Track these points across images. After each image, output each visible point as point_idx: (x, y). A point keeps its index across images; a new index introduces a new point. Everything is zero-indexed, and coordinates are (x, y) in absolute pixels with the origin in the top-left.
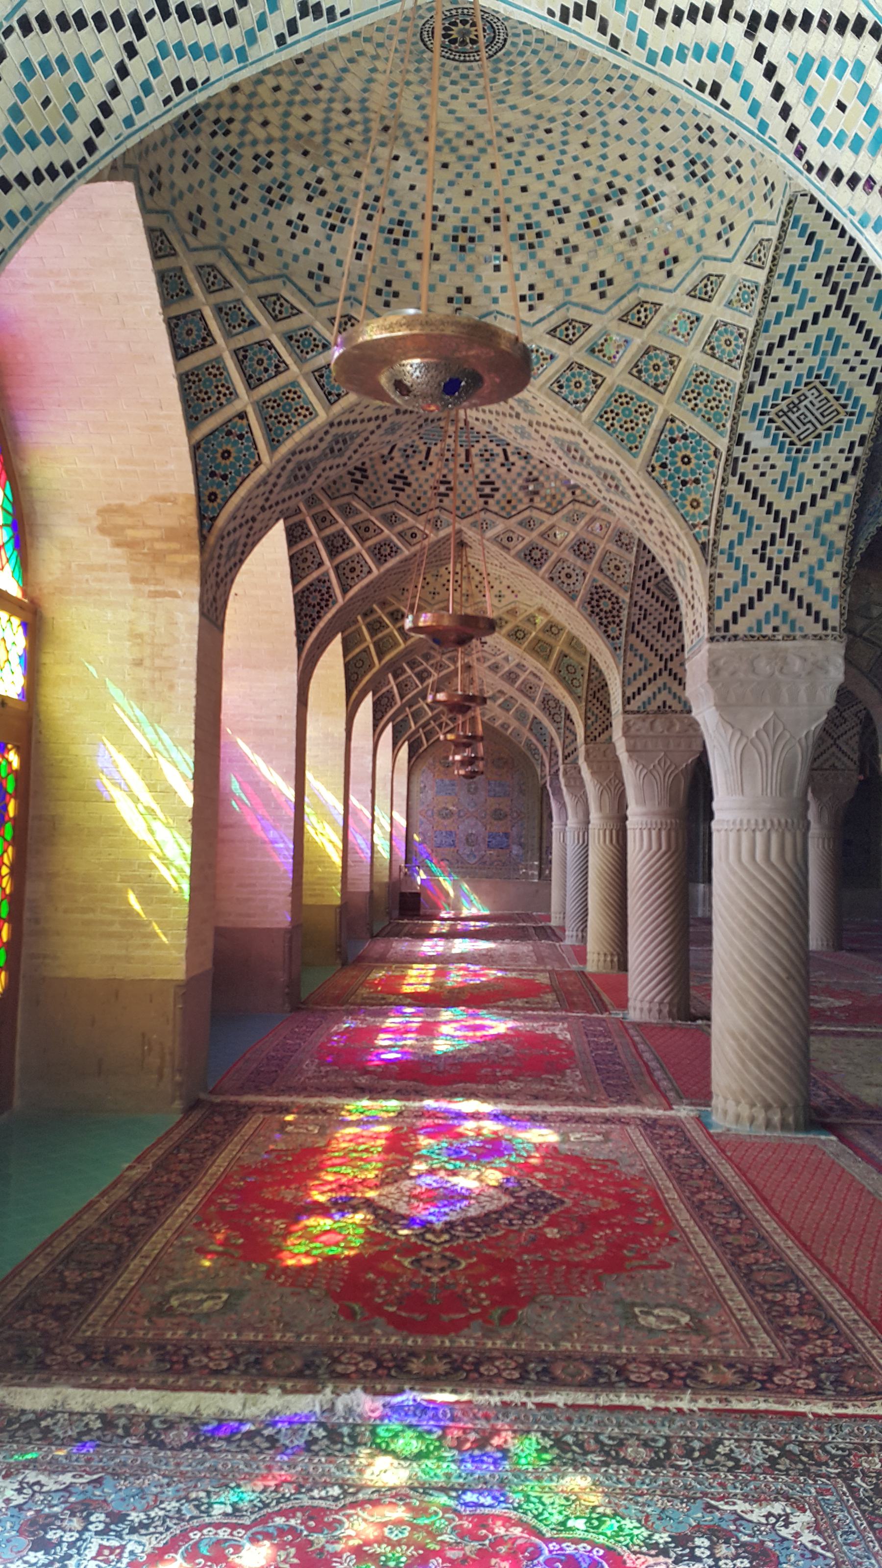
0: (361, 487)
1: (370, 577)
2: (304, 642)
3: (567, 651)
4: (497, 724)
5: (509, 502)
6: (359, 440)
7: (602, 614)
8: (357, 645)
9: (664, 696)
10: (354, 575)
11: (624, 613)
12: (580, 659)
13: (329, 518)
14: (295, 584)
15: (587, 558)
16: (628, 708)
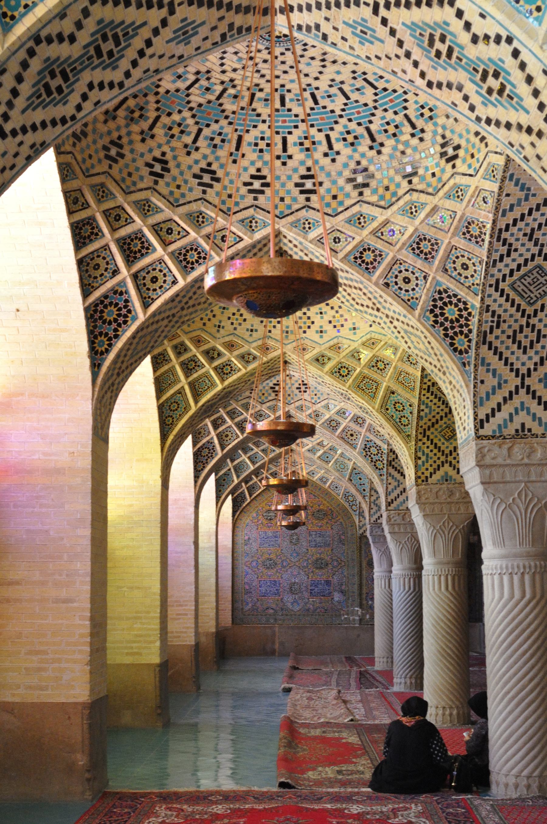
0: (161, 182)
1: (176, 289)
2: (100, 366)
3: (394, 387)
4: (316, 478)
5: (335, 197)
6: (138, 43)
7: (448, 324)
8: (170, 385)
9: (522, 417)
10: (156, 286)
11: (474, 322)
12: (408, 396)
13: (124, 216)
14: (86, 294)
15: (428, 257)
16: (482, 432)
